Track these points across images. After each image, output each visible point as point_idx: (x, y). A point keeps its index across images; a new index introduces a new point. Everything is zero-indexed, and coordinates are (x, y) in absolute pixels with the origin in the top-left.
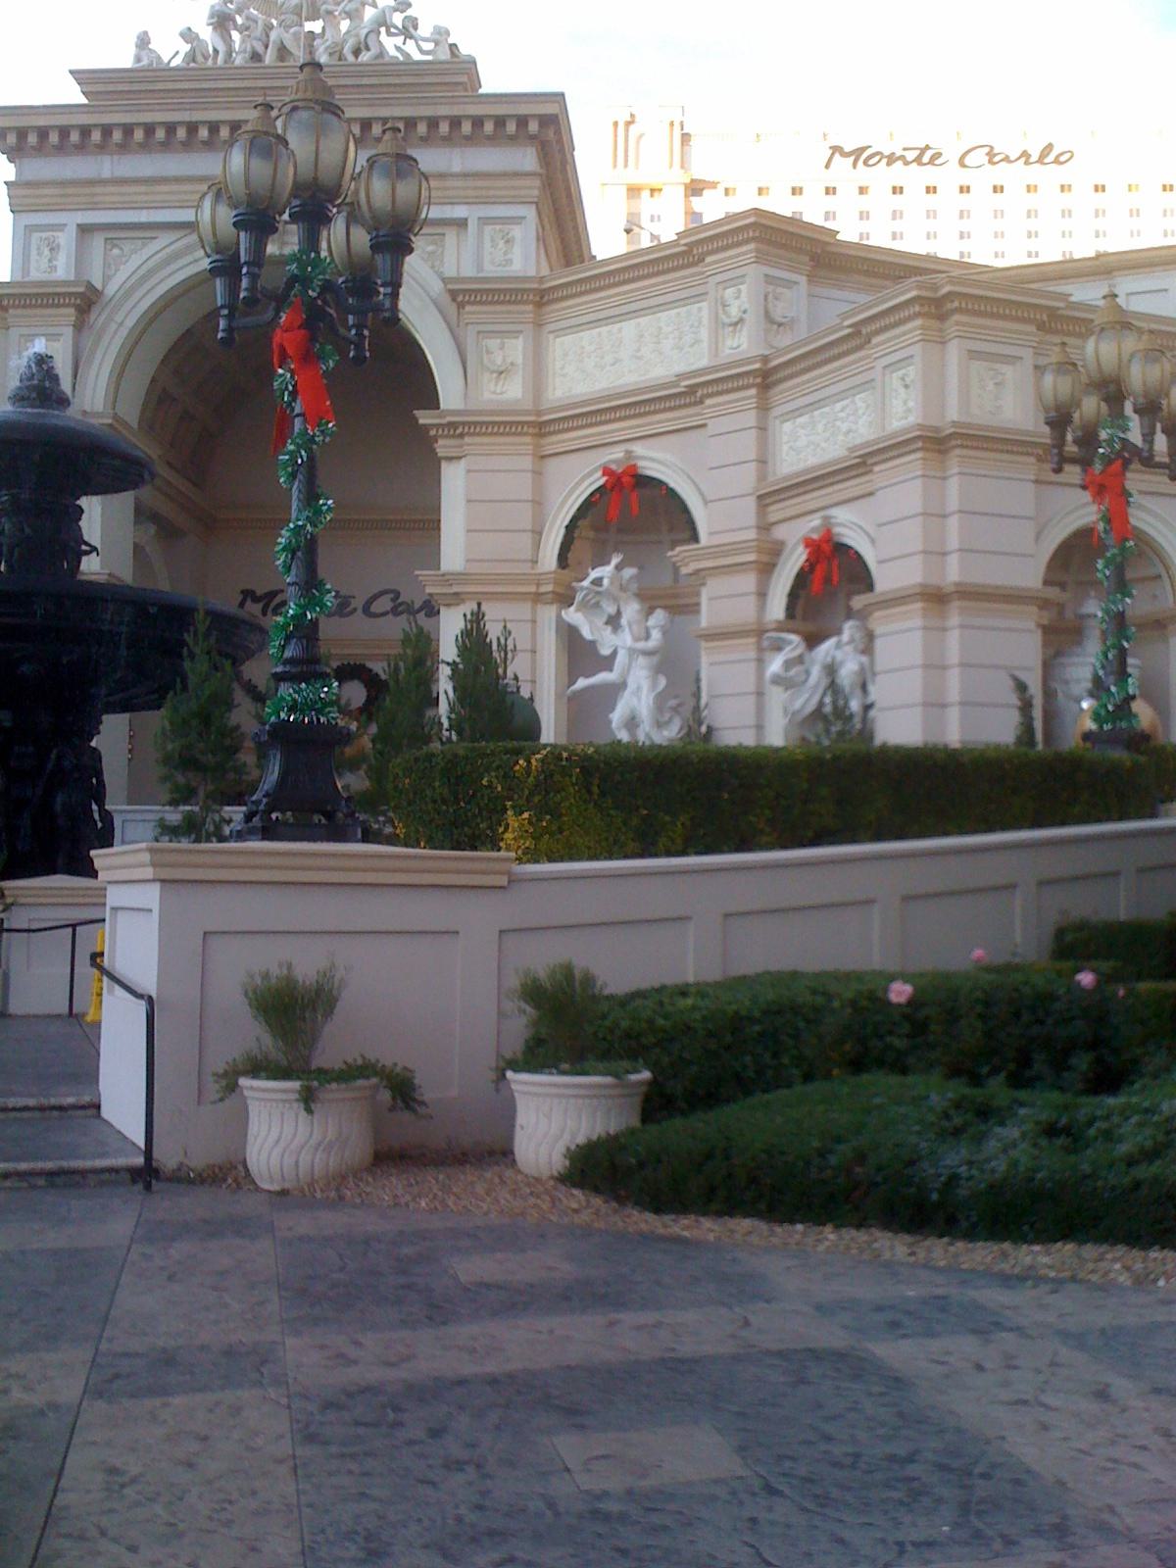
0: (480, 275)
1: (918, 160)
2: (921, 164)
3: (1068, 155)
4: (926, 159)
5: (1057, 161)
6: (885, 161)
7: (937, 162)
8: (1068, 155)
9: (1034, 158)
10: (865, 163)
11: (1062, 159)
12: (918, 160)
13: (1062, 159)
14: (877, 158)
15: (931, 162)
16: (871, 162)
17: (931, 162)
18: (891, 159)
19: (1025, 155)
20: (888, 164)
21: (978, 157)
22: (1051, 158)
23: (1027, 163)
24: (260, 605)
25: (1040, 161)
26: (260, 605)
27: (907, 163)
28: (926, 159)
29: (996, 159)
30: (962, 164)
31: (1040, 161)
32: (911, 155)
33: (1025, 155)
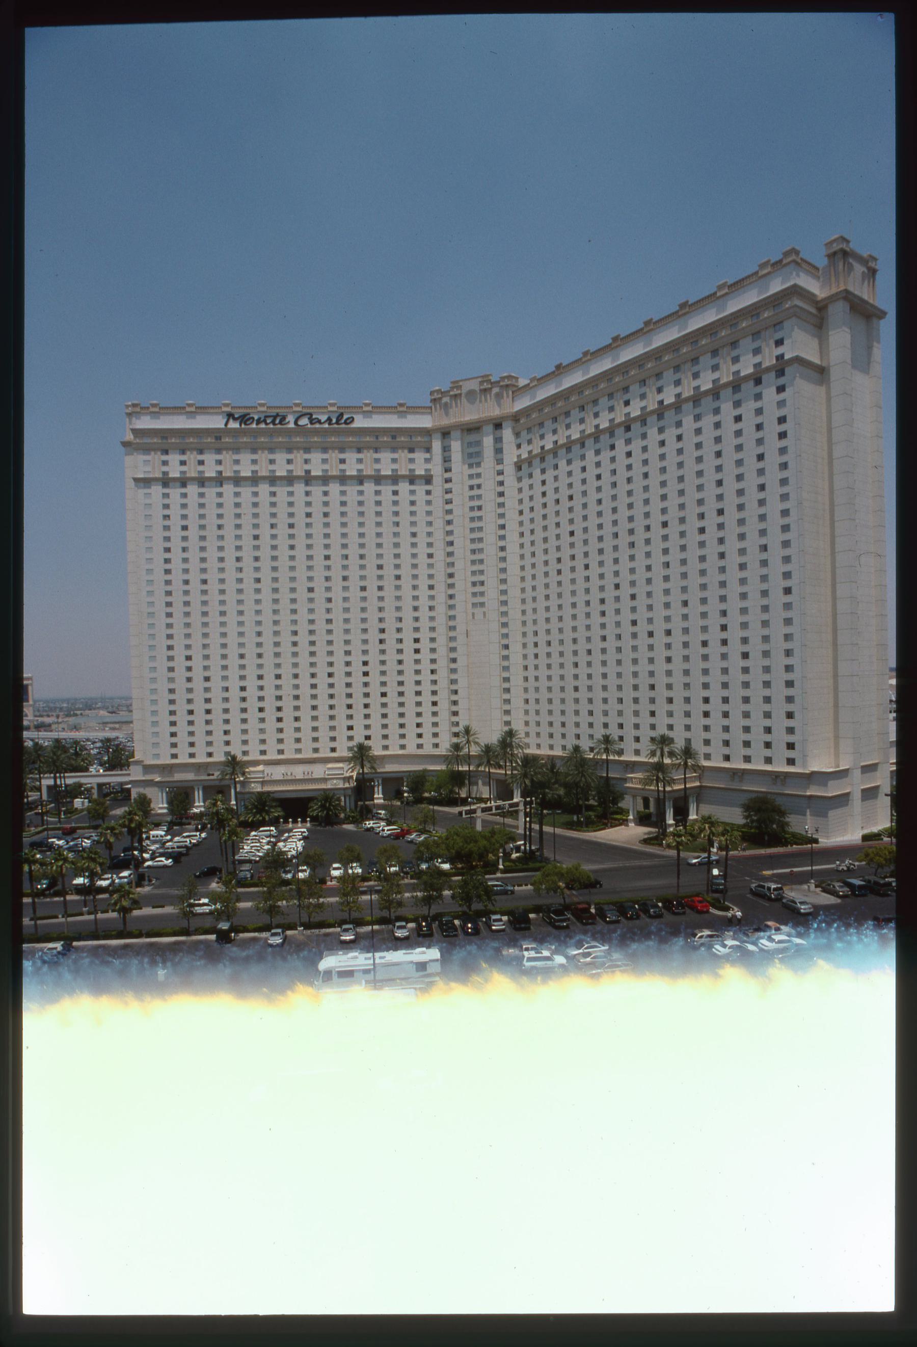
1: (273, 422)
4: (277, 421)
5: (345, 423)
6: (255, 422)
10: (245, 424)
11: (348, 421)
13: (348, 421)
14: (251, 420)
15: (280, 423)
16: (248, 422)
17: (280, 423)
20: (257, 424)
21: (304, 421)
22: (343, 421)
23: (330, 424)
28: (277, 421)
30: (296, 423)
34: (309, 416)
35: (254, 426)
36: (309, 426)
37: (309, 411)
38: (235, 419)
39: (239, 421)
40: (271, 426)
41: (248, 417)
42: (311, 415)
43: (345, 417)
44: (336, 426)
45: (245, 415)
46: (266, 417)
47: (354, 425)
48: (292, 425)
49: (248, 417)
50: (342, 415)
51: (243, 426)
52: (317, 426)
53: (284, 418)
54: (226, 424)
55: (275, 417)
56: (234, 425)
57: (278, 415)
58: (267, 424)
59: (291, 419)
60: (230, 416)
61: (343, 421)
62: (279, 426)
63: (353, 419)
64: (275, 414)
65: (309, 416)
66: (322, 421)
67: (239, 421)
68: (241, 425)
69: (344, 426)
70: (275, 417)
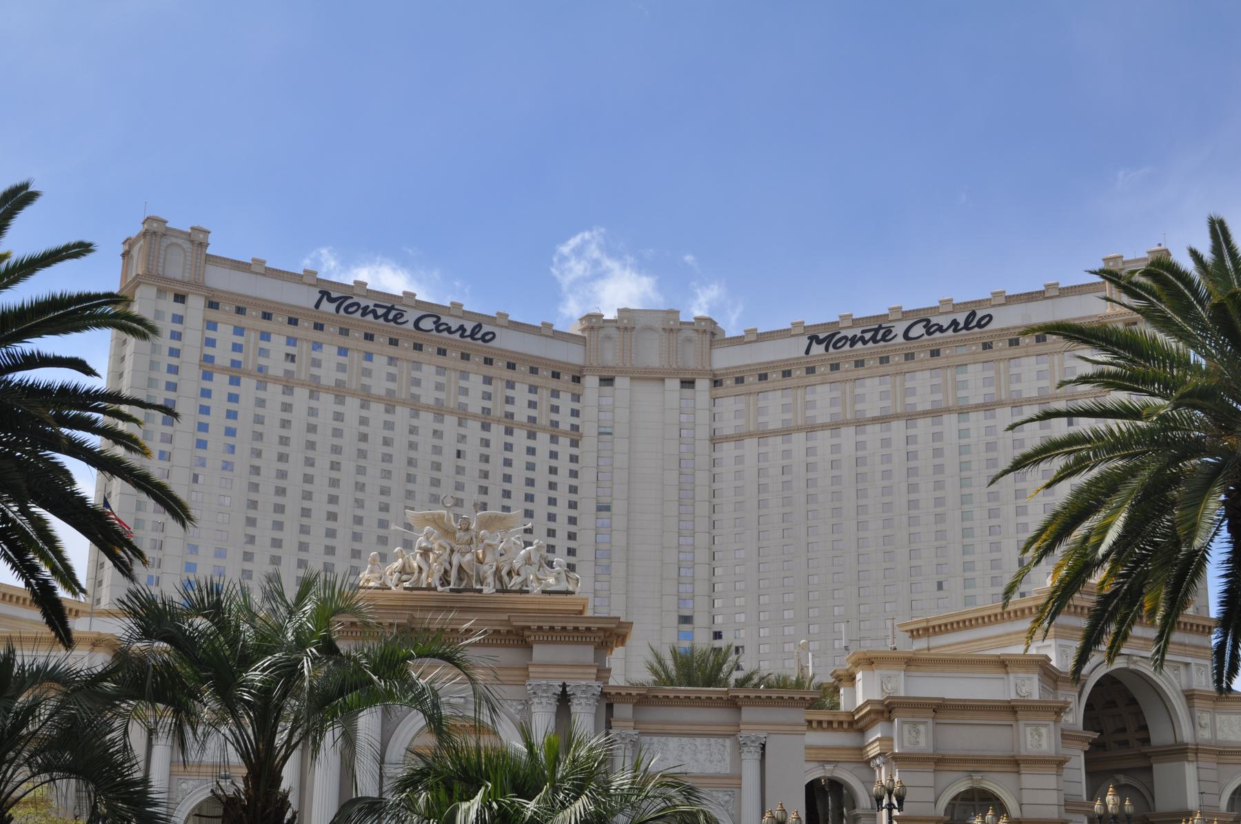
0: (596, 615)
1: (874, 339)
2: (875, 341)
3: (987, 319)
4: (879, 337)
5: (979, 325)
6: (849, 343)
7: (888, 338)
8: (987, 319)
9: (962, 325)
10: (835, 347)
11: (983, 322)
12: (874, 339)
13: (983, 322)
14: (844, 341)
17: (884, 339)
18: (853, 341)
19: (955, 323)
20: (851, 346)
21: (918, 330)
22: (974, 323)
23: (955, 330)
24: (335, 305)
25: (966, 327)
26: (335, 305)
27: (865, 342)
28: (879, 337)
29: (932, 330)
31: (966, 327)
32: (868, 336)
33: (955, 323)
34: (925, 323)
35: (847, 347)
36: (926, 337)
37: (923, 316)
38: (819, 342)
39: (825, 344)
40: (871, 344)
41: (838, 337)
42: (928, 321)
43: (980, 314)
44: (964, 332)
45: (833, 335)
46: (863, 332)
47: (993, 326)
48: (900, 339)
49: (838, 337)
50: (973, 314)
51: (831, 349)
52: (938, 334)
53: (889, 331)
54: (807, 352)
55: (876, 331)
56: (817, 349)
57: (880, 327)
58: (865, 342)
59: (899, 329)
60: (814, 339)
61: (974, 323)
62: (882, 343)
63: (990, 317)
64: (877, 326)
65: (925, 323)
66: (945, 327)
67: (825, 344)
68: (827, 349)
69: (976, 330)
70: (876, 331)
